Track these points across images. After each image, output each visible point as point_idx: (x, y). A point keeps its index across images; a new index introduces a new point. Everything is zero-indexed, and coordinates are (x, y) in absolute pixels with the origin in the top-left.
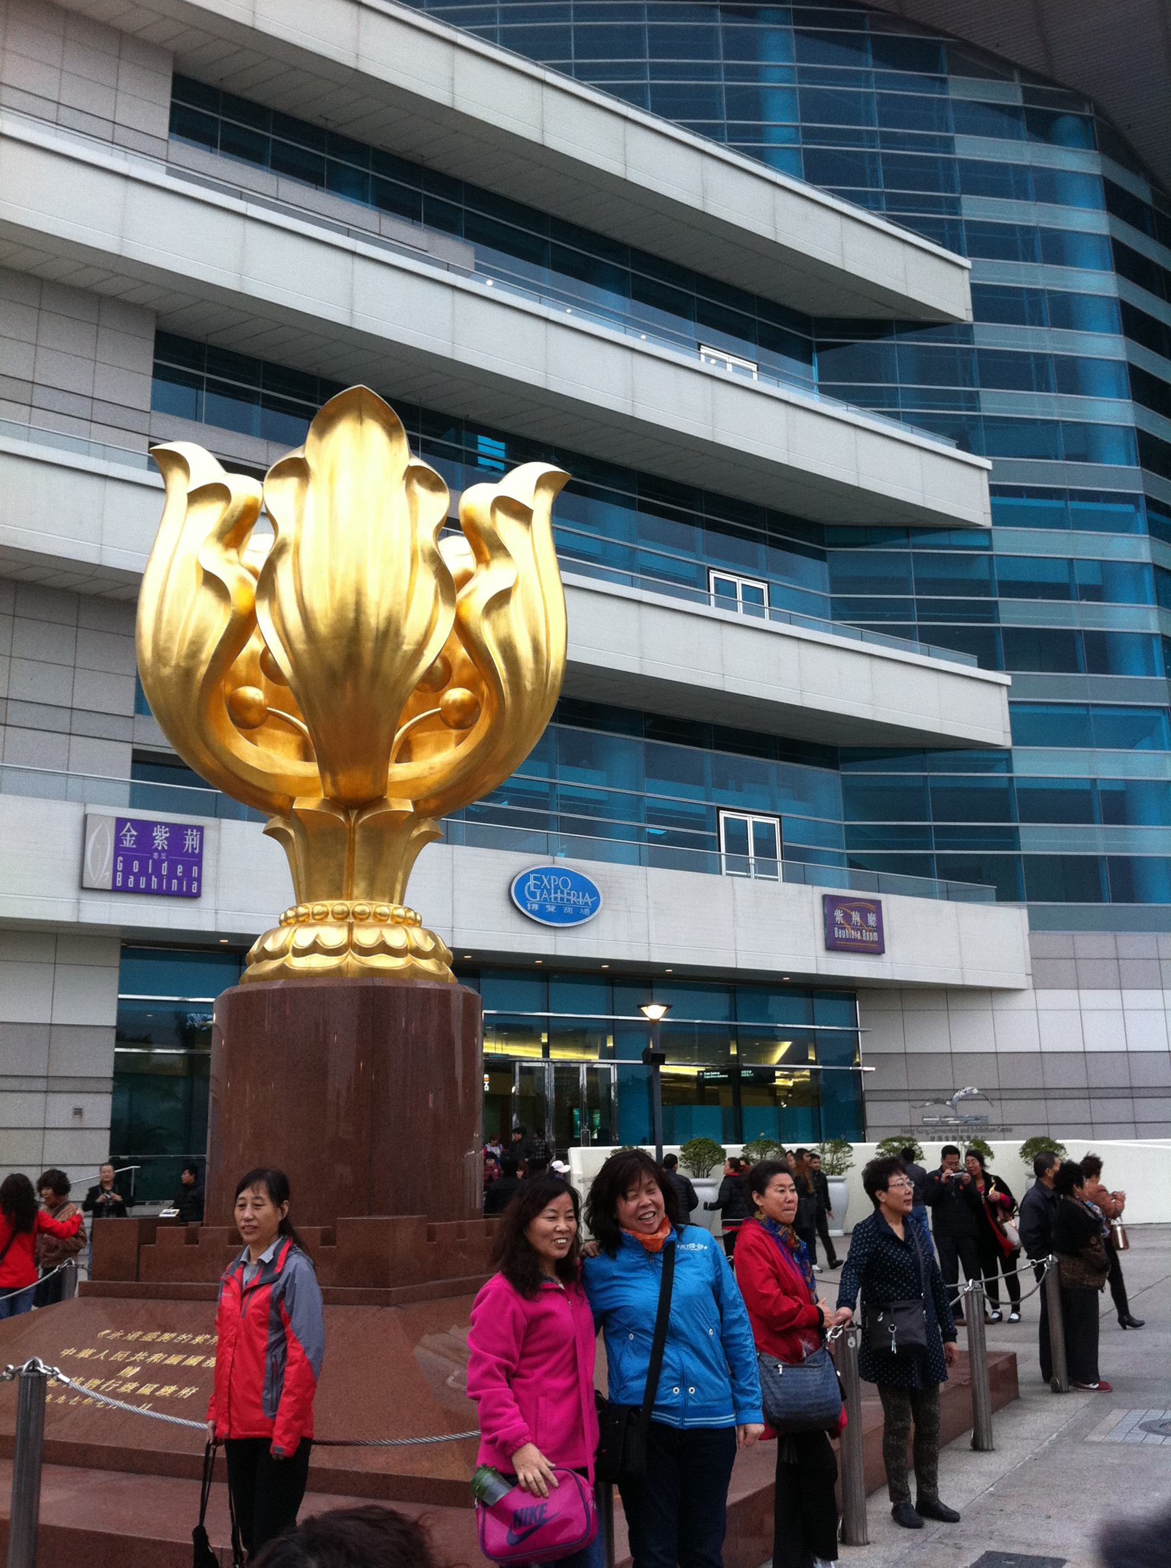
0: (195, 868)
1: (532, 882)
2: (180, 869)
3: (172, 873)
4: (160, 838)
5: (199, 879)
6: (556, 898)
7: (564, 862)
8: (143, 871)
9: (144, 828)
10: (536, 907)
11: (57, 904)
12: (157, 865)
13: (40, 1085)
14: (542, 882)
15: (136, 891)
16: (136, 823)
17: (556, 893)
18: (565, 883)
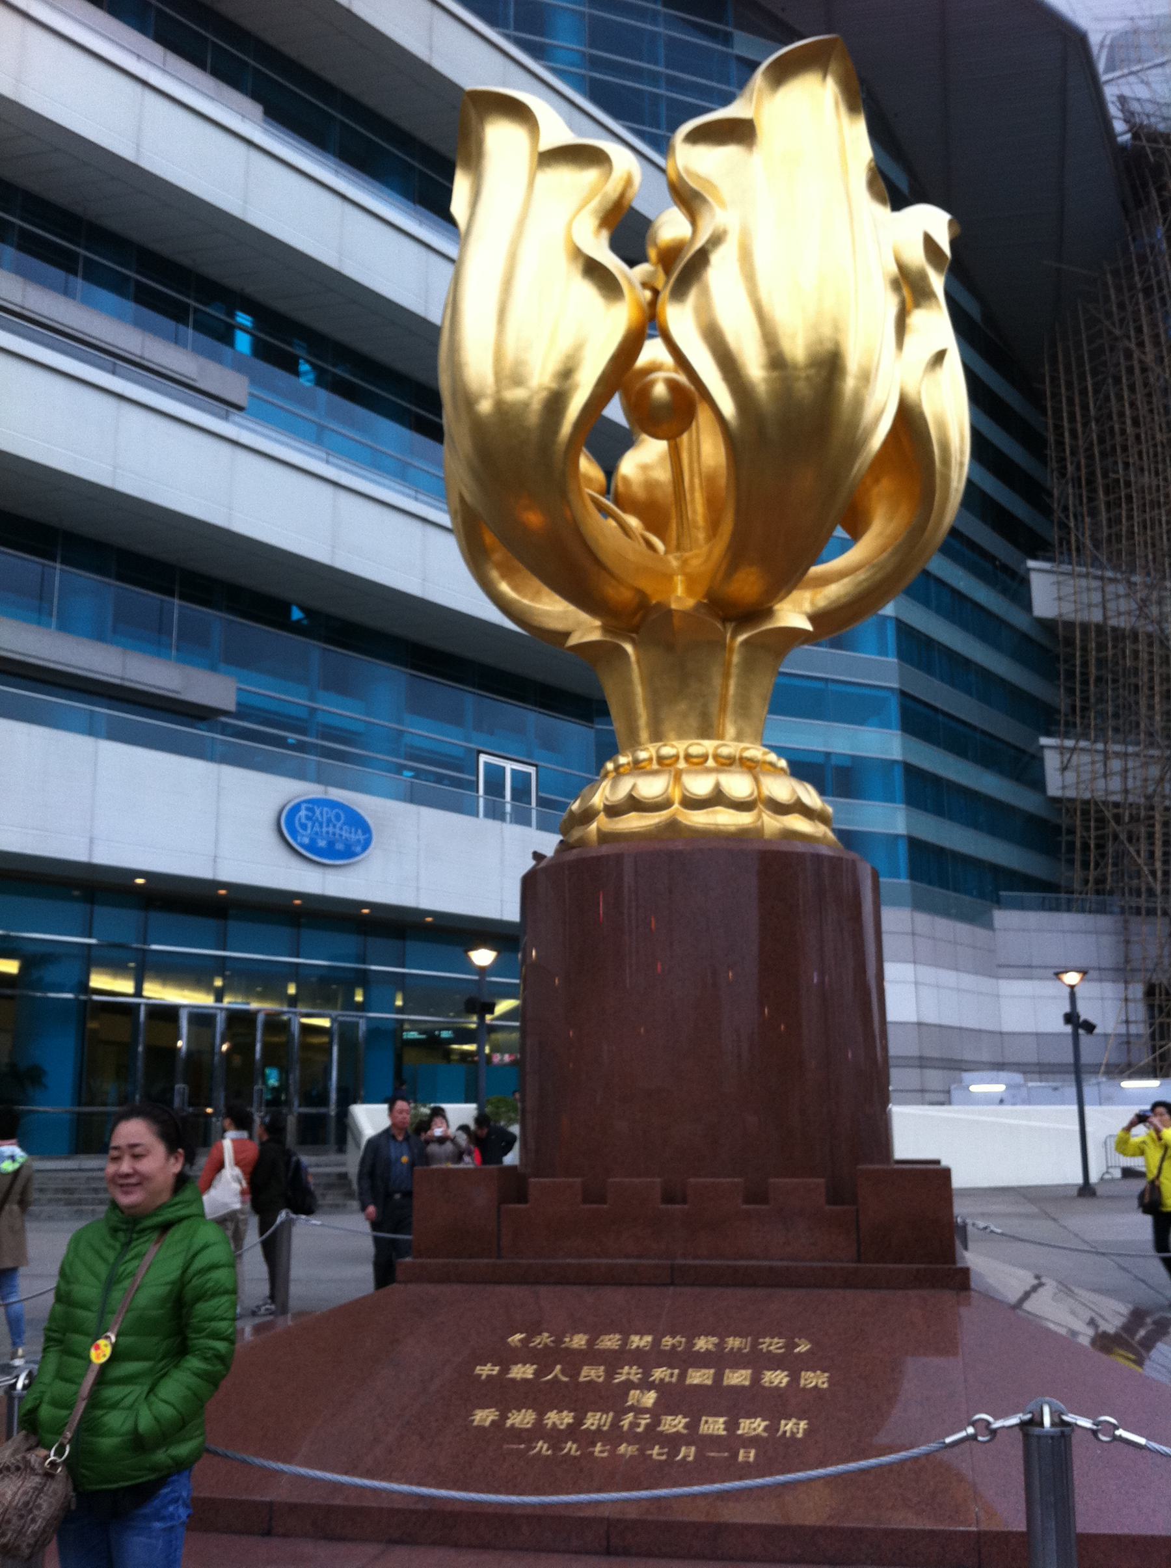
1: (303, 813)
6: (328, 833)
7: (337, 794)
10: (306, 840)
17: (328, 826)
18: (338, 817)
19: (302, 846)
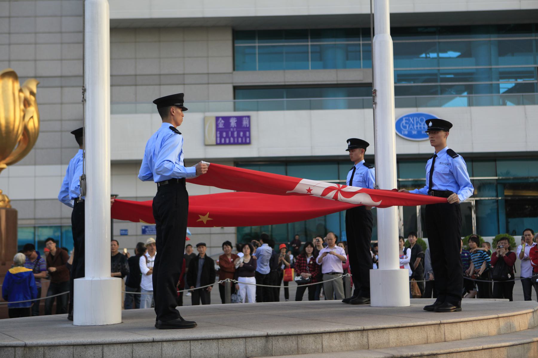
0: (248, 133)
1: (404, 122)
2: (242, 134)
3: (238, 135)
4: (233, 122)
5: (249, 137)
8: (227, 136)
9: (227, 119)
10: (406, 133)
14: (409, 120)
15: (225, 144)
16: (224, 118)
17: (417, 124)
19: (404, 135)
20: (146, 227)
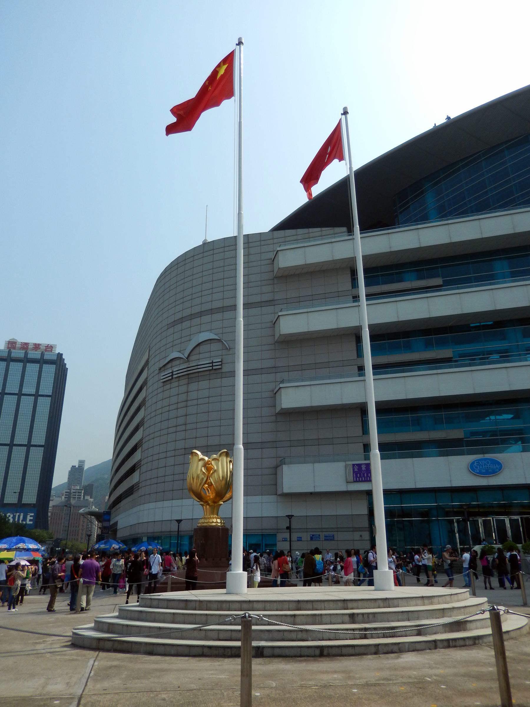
4: (364, 468)
7: (487, 456)
8: (360, 476)
9: (359, 466)
11: (343, 488)
12: (364, 474)
13: (351, 529)
15: (359, 481)
16: (358, 465)
18: (488, 463)
20: (313, 535)
